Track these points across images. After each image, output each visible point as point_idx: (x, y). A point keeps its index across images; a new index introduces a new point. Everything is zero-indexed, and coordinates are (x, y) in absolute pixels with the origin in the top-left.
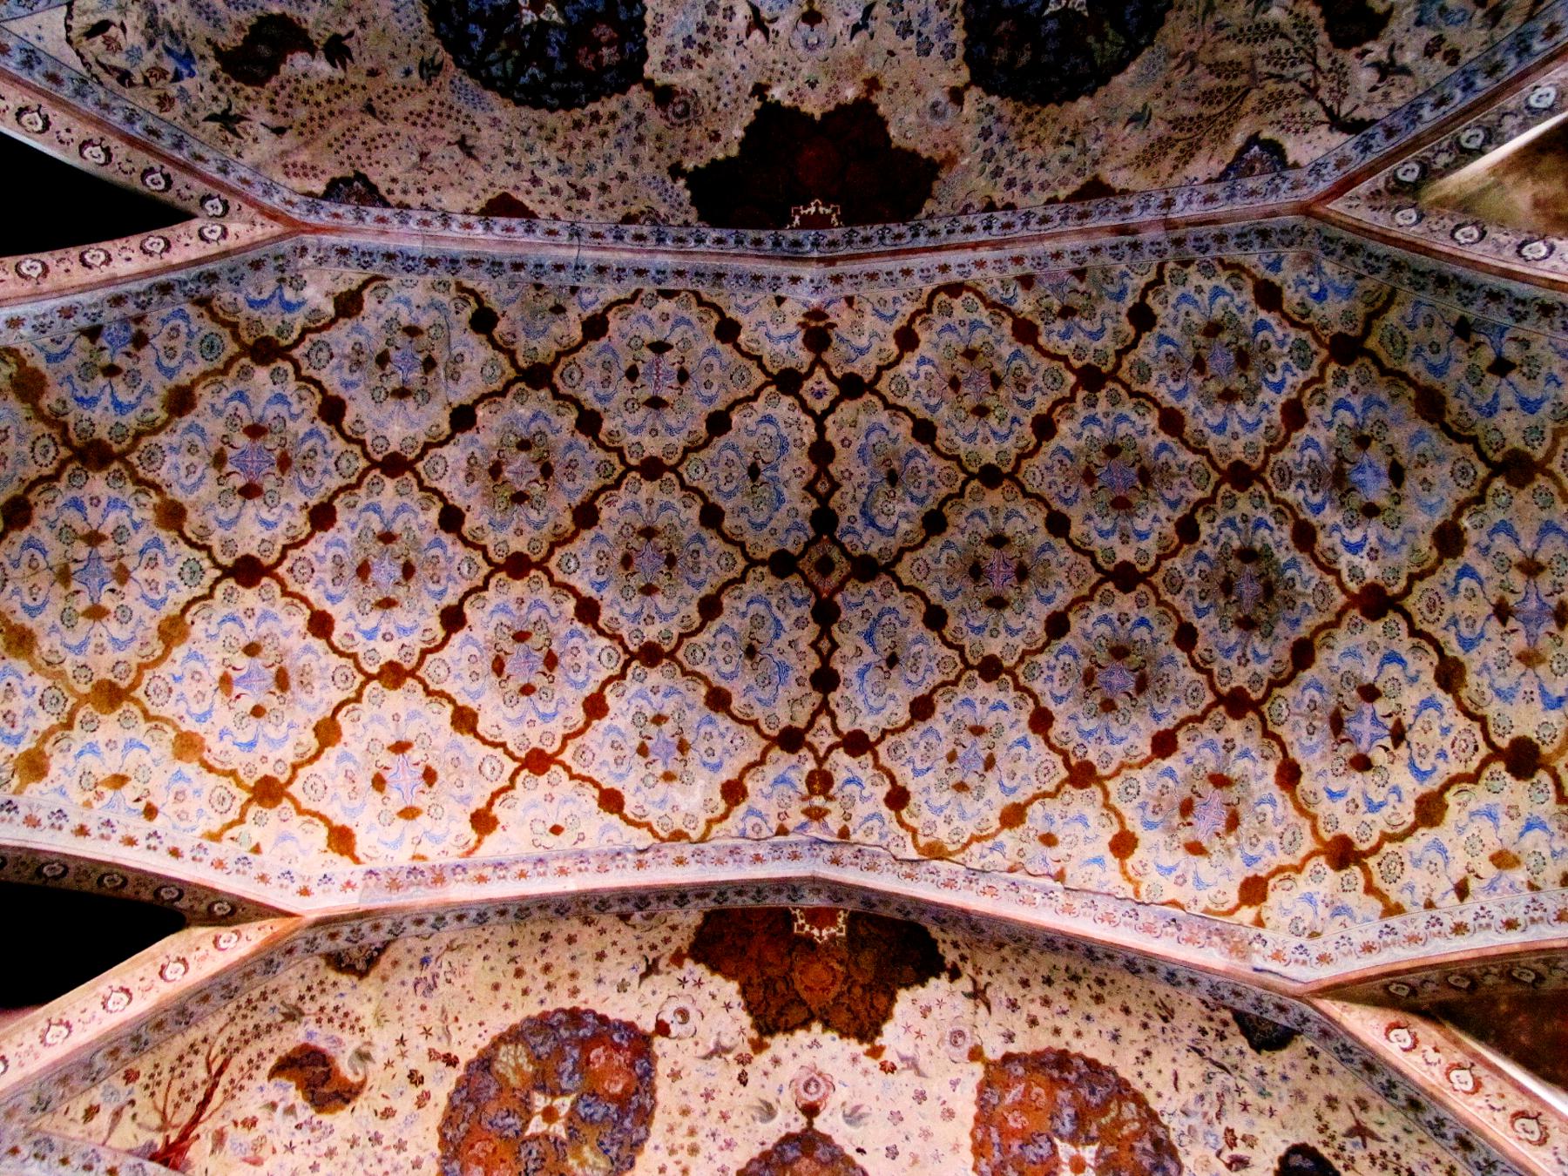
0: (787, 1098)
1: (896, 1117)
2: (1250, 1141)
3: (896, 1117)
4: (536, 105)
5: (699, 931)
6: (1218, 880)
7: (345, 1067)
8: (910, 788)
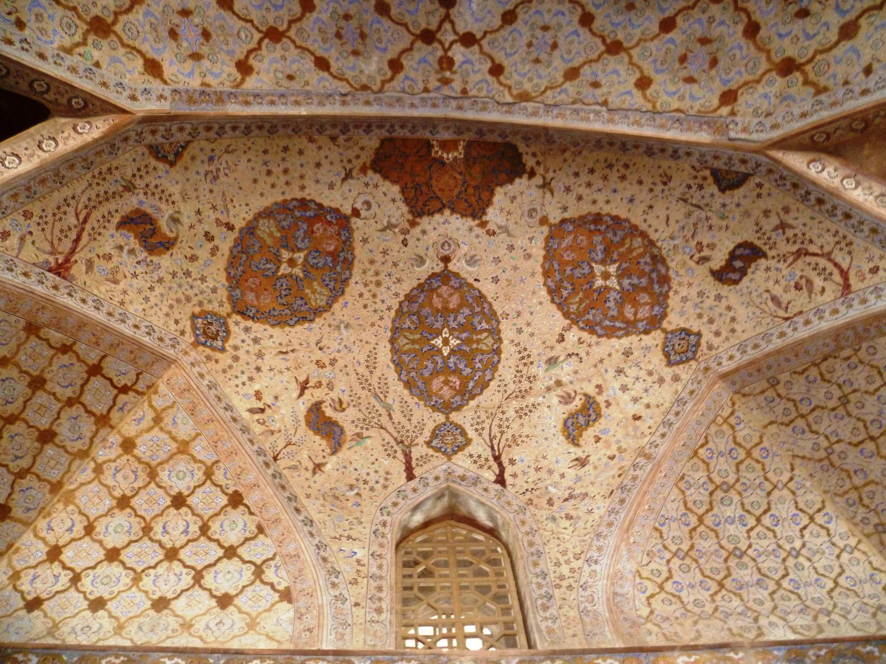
0: (431, 252)
1: (497, 260)
2: (712, 246)
3: (497, 260)
5: (377, 152)
6: (706, 96)
7: (164, 225)
8: (505, 63)
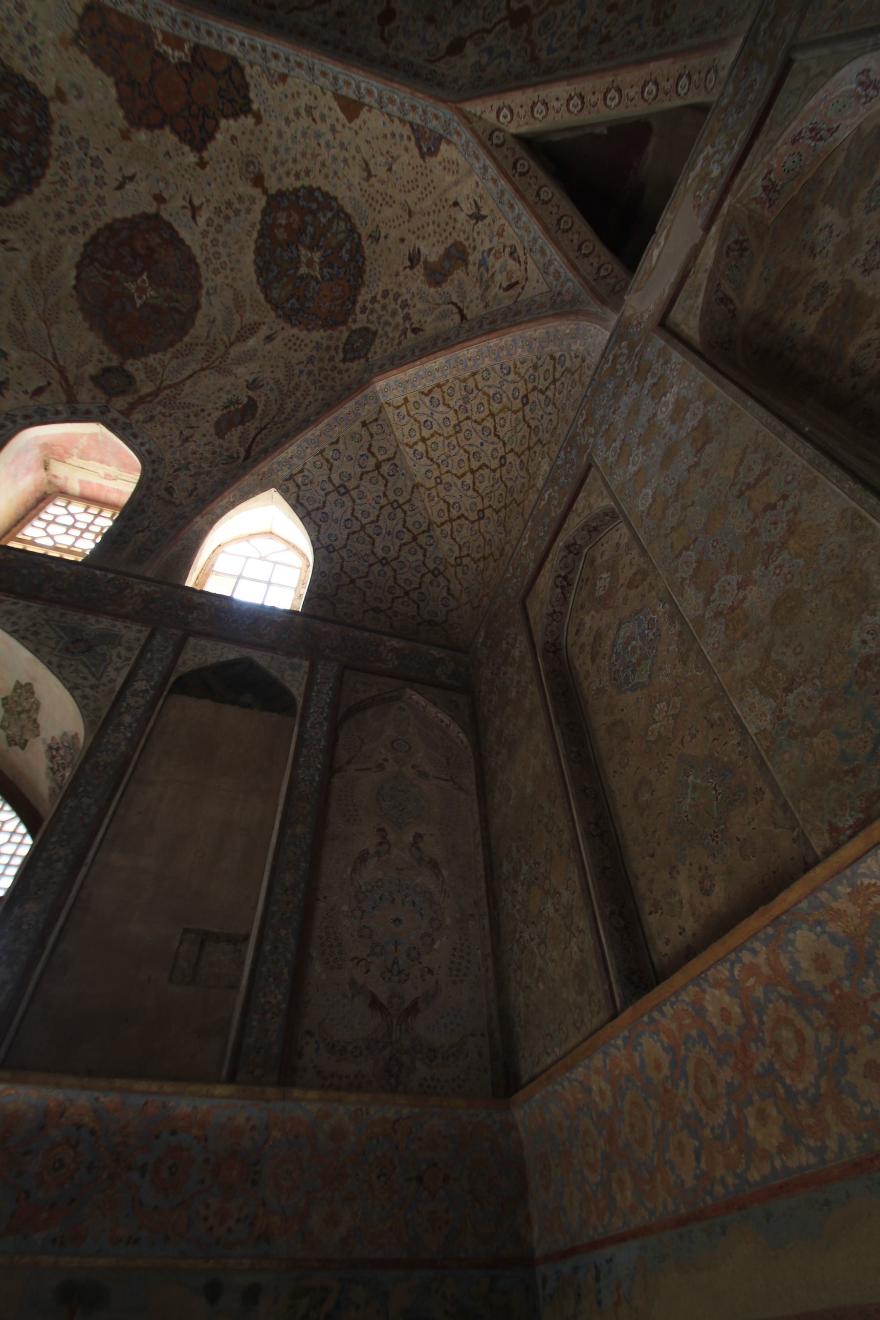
4: (326, 195)
